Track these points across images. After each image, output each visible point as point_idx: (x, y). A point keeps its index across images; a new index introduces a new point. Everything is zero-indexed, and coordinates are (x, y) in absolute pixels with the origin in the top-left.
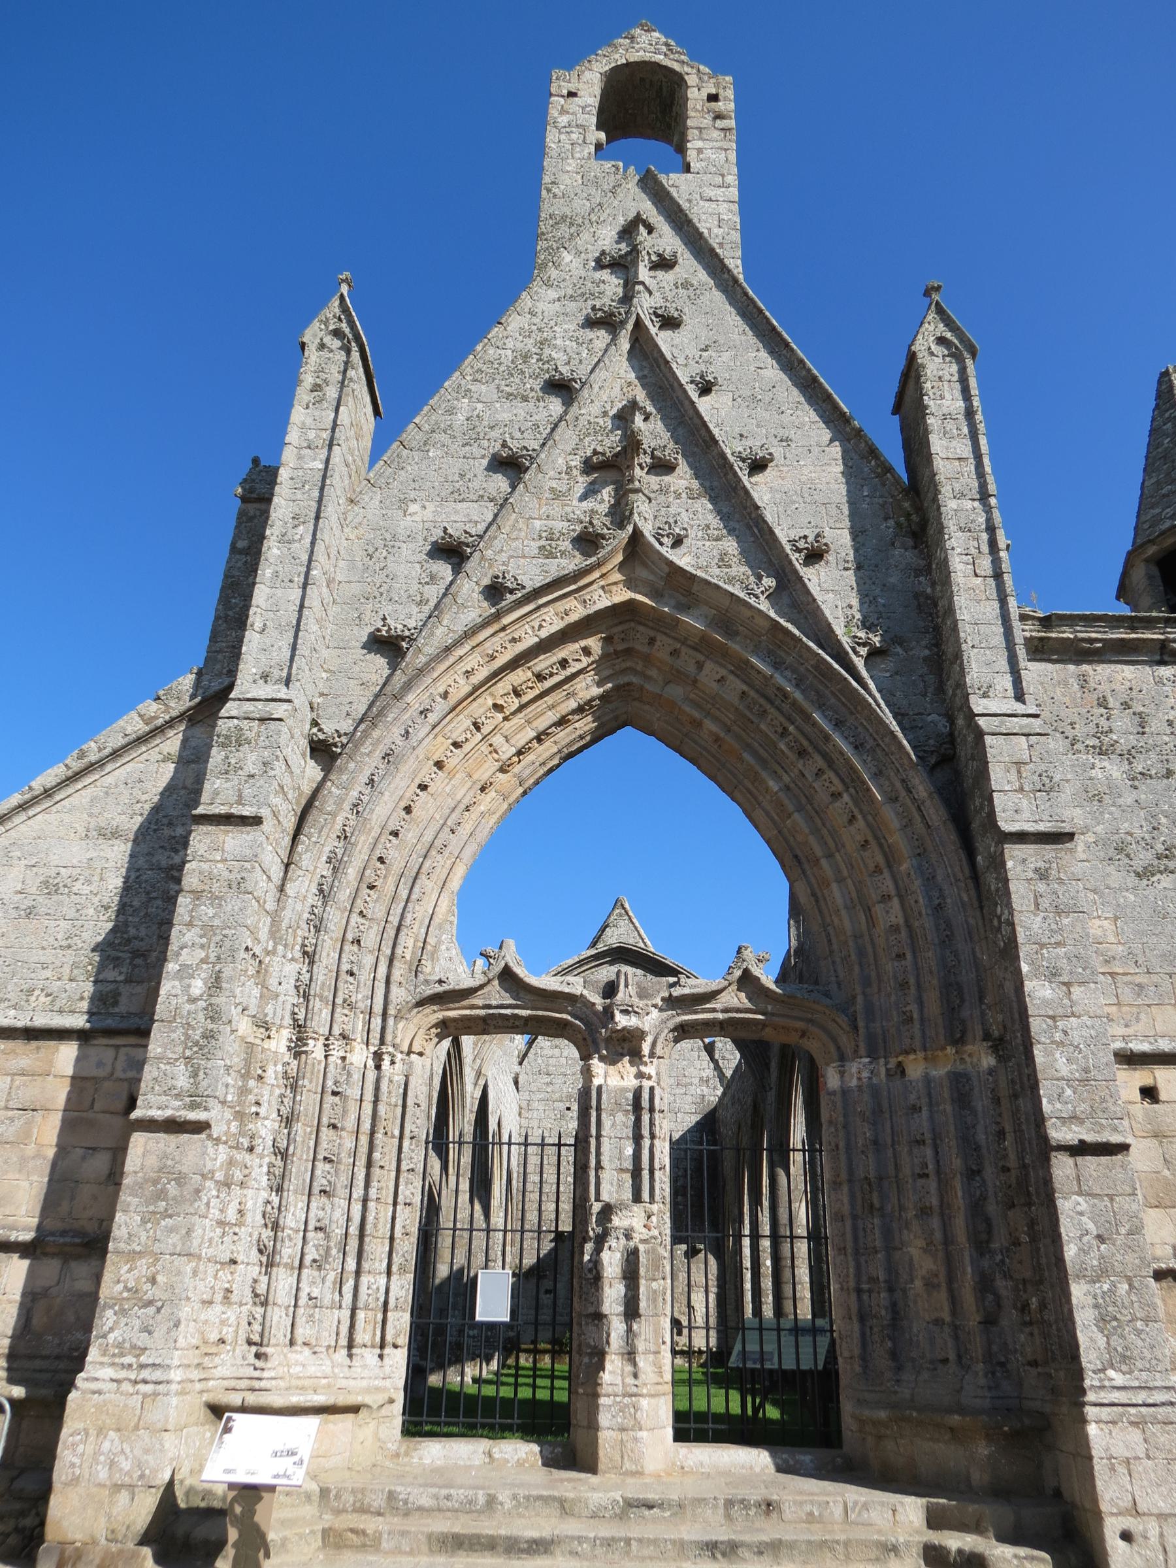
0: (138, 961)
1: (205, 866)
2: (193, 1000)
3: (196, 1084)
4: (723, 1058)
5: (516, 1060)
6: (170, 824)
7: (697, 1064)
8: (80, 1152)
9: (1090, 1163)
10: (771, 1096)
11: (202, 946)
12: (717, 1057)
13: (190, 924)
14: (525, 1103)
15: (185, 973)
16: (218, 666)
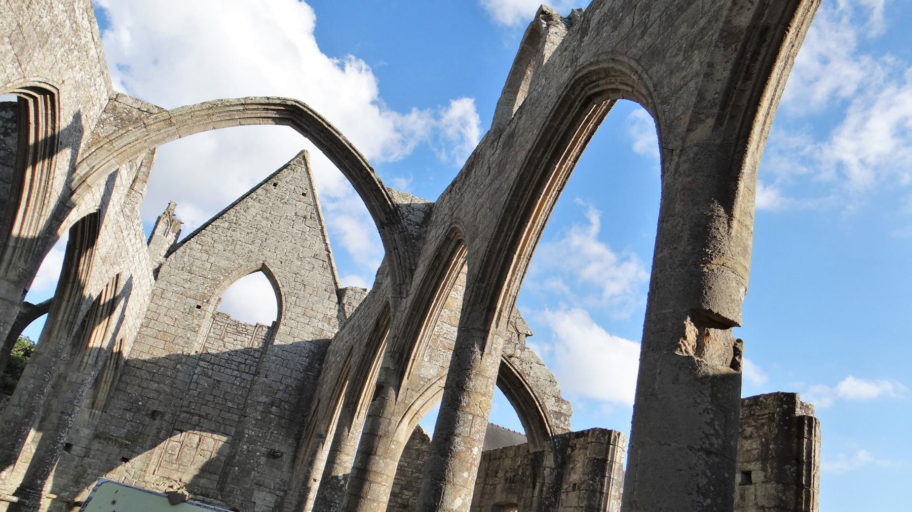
4: (350, 304)
5: (164, 253)
7: (326, 303)
10: (407, 303)
12: (345, 301)
14: (160, 290)
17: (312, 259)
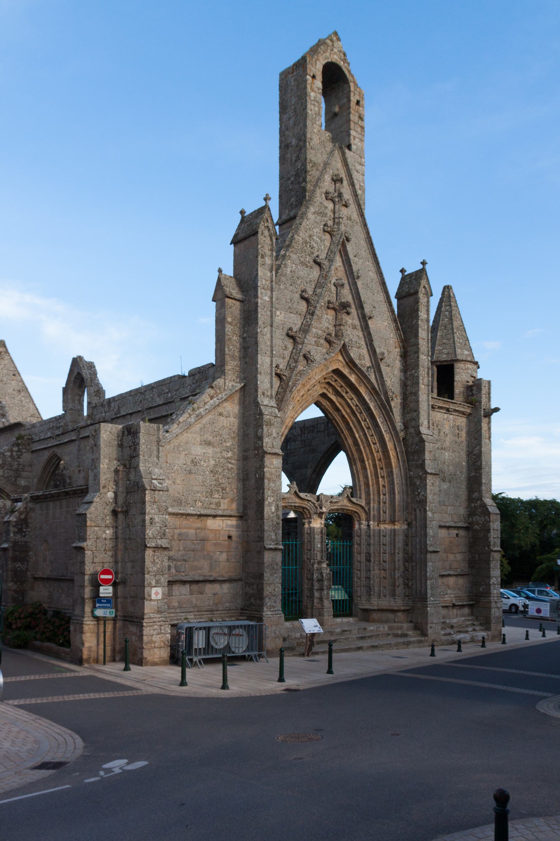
0: (224, 491)
1: (270, 470)
2: (273, 513)
3: (277, 538)
6: (225, 441)
8: (218, 553)
9: (433, 555)
11: (273, 496)
13: (269, 489)
15: (270, 504)
16: (230, 377)
17: (32, 418)
